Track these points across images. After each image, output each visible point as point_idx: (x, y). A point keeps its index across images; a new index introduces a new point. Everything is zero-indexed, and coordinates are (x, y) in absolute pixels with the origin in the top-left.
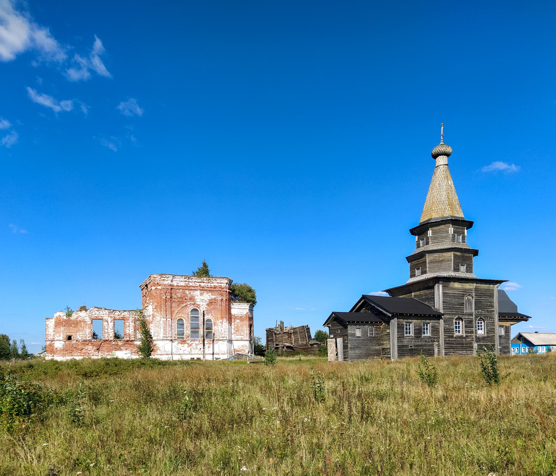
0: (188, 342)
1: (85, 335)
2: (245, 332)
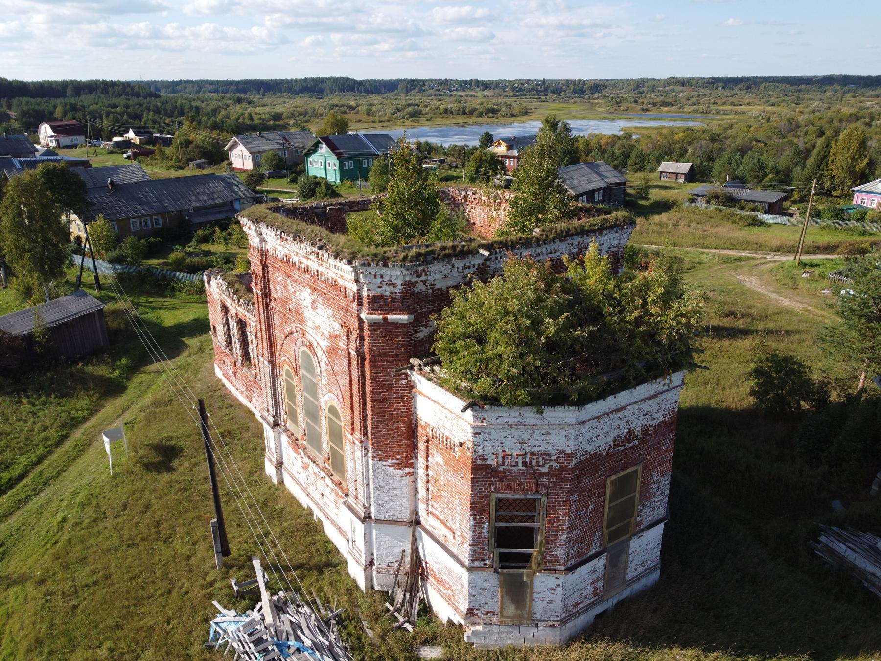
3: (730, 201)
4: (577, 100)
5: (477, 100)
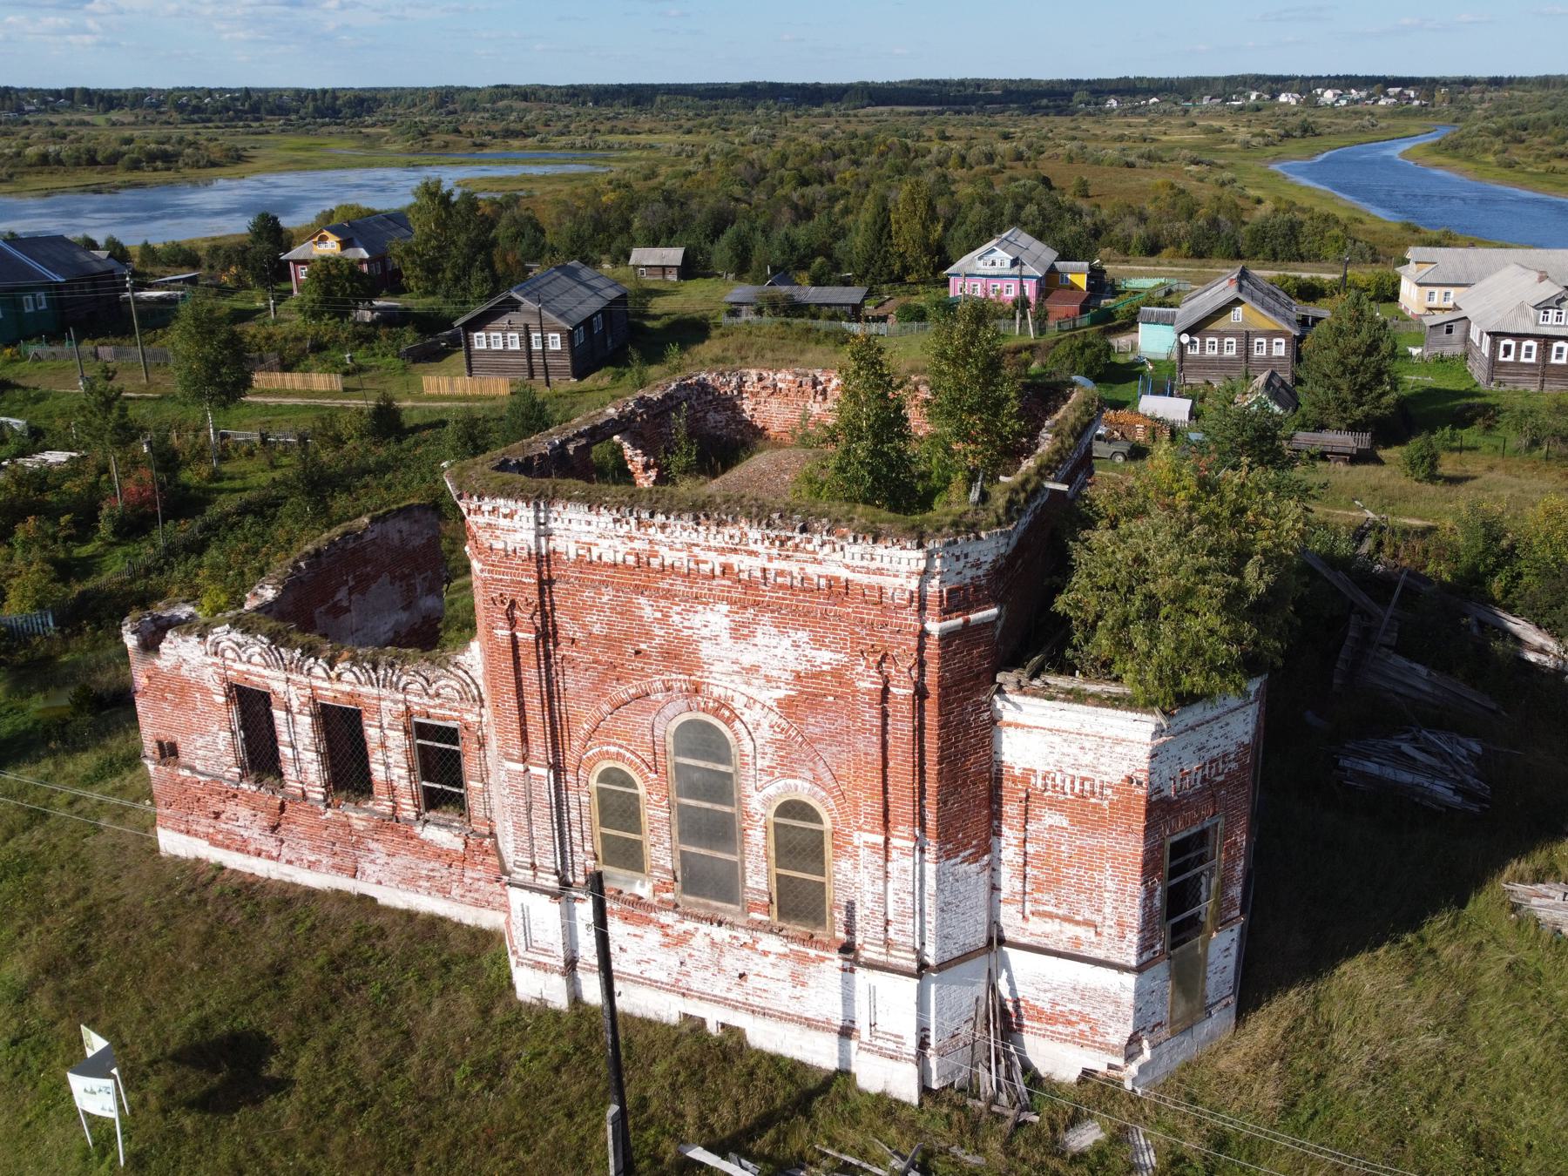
2: (1107, 910)
3: (796, 308)
4: (334, 129)
5: (103, 130)
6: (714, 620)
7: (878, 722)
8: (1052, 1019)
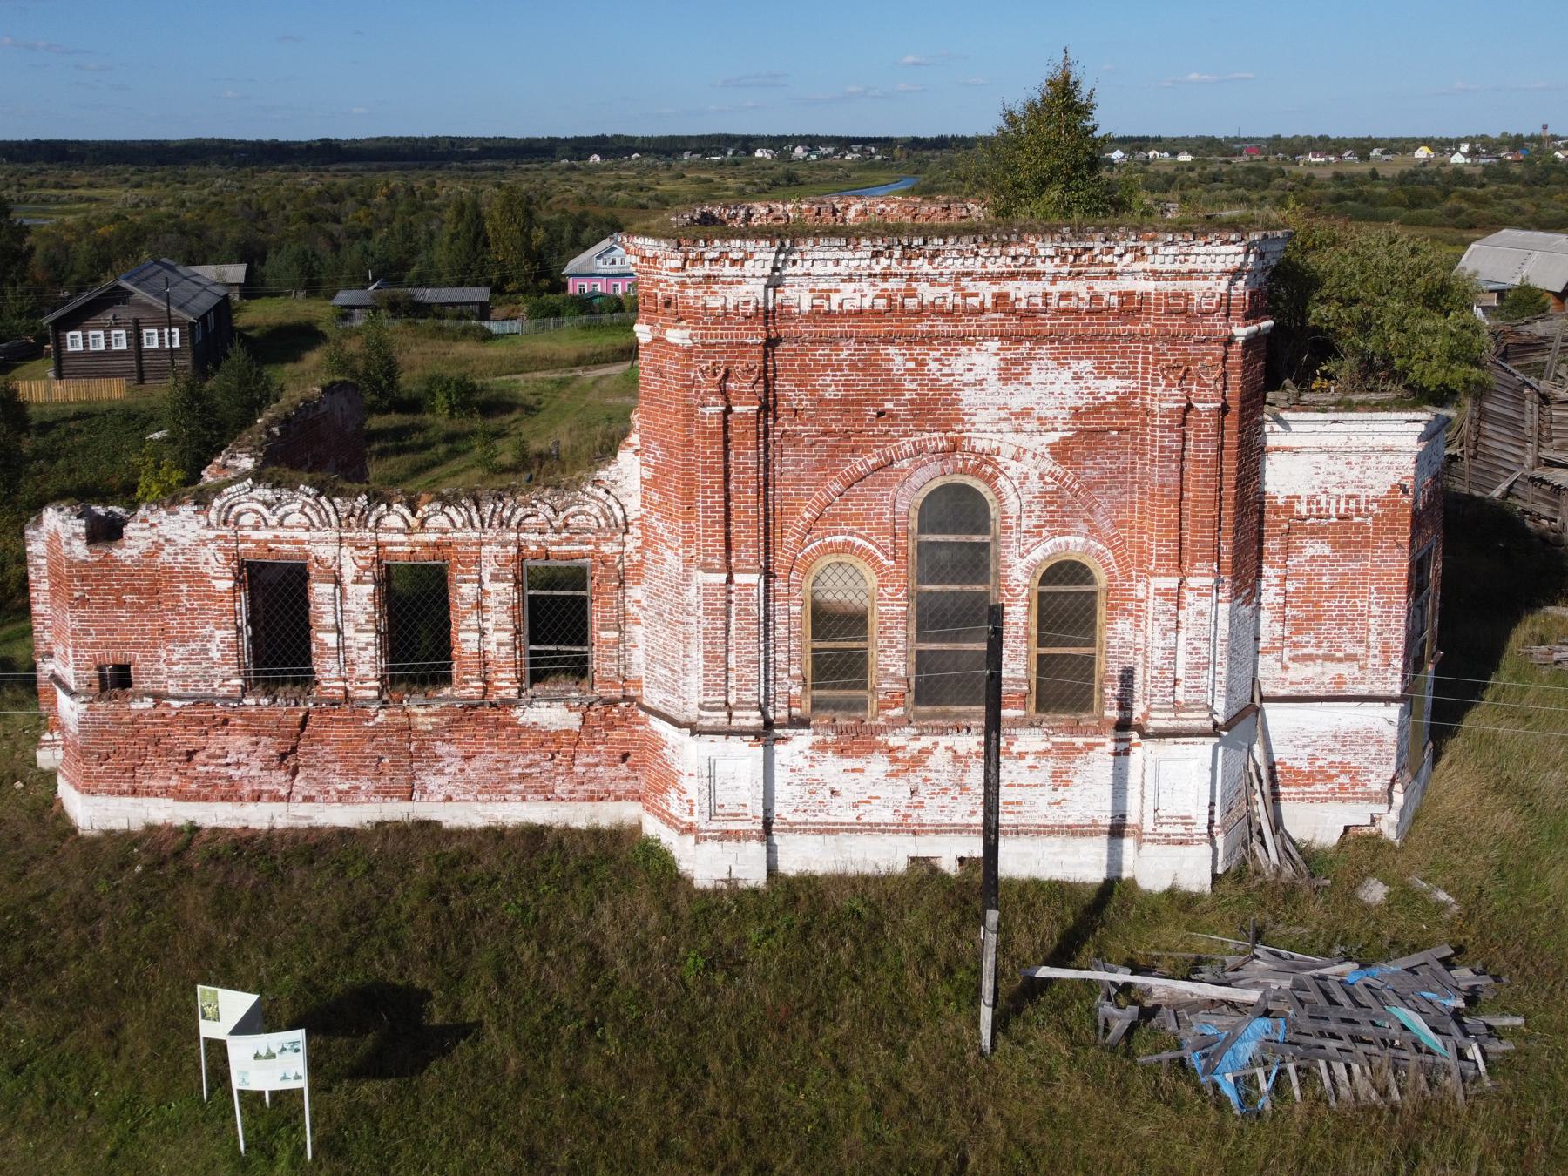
0: (893, 741)
1: (205, 664)
2: (1372, 638)
6: (985, 359)
7: (1177, 447)
8: (1310, 779)
